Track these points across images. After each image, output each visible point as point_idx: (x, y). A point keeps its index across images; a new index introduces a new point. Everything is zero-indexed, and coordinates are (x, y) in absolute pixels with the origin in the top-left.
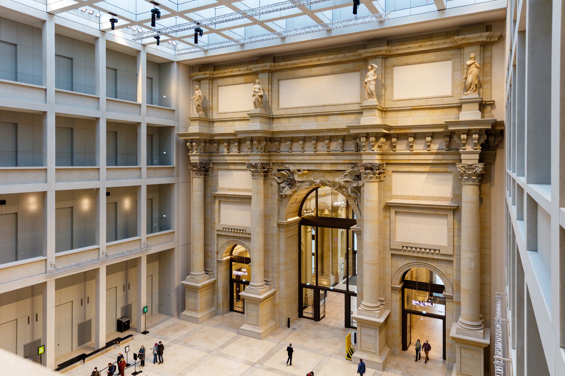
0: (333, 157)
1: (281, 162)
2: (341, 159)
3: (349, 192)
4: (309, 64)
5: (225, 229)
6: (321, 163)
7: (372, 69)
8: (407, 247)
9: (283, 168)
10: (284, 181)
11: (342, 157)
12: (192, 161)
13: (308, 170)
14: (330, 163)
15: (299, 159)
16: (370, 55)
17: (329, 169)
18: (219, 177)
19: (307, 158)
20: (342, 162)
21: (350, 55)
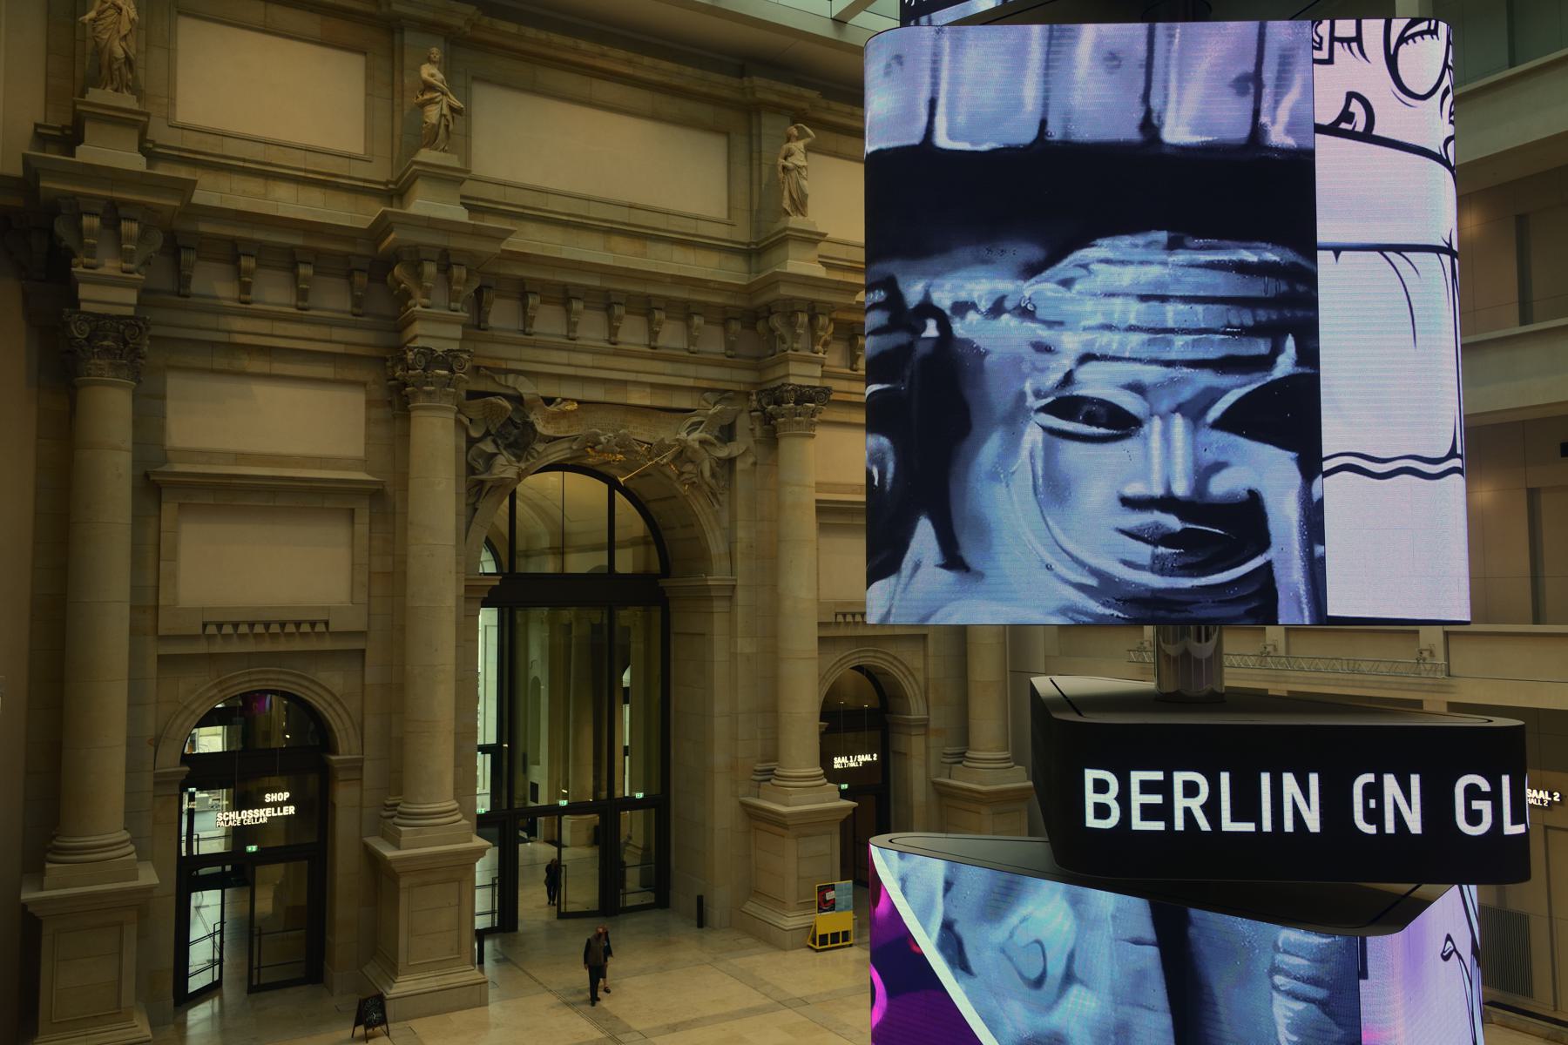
0: (668, 367)
1: (488, 363)
2: (689, 375)
3: (707, 473)
4: (600, 63)
5: (218, 626)
6: (625, 383)
7: (798, 139)
8: (844, 615)
9: (489, 386)
10: (487, 433)
11: (691, 370)
12: (84, 307)
13: (579, 402)
14: (653, 385)
15: (558, 361)
16: (775, 98)
17: (647, 402)
18: (171, 405)
19: (586, 359)
20: (691, 383)
21: (721, 83)
